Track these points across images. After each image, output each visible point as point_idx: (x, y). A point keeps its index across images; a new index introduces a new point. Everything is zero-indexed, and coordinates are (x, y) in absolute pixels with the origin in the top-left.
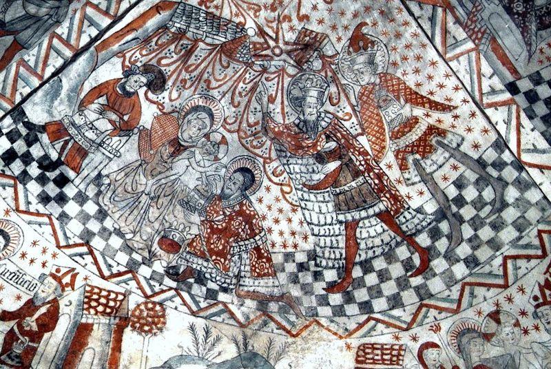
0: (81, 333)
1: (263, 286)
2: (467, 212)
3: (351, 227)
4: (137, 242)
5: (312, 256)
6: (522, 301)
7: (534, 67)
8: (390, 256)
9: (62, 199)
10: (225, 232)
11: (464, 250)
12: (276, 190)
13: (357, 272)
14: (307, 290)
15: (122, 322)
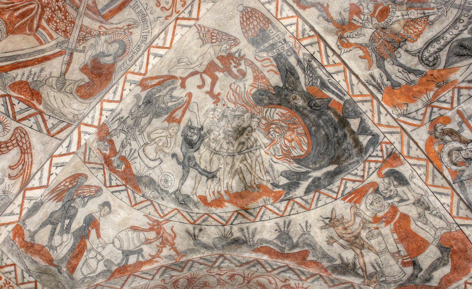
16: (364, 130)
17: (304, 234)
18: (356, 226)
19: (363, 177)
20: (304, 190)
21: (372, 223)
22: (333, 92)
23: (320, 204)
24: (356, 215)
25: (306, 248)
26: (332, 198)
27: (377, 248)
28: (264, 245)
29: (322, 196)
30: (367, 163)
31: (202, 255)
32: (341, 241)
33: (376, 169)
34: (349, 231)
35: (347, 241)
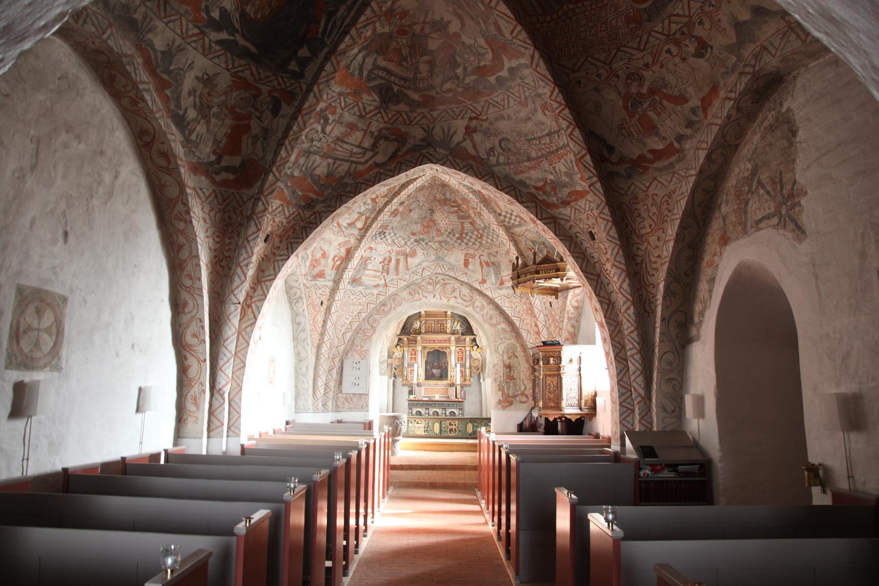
0: (398, 261)
1: (440, 239)
2: (491, 231)
3: (462, 224)
4: (405, 237)
5: (452, 230)
6: (503, 252)
7: (506, 210)
8: (472, 233)
9: (385, 237)
10: (428, 226)
11: (490, 237)
12: (440, 213)
13: (464, 235)
14: (451, 239)
15: (406, 256)
16: (303, 63)
17: (181, 69)
18: (217, 100)
19: (261, 80)
20: (219, 39)
21: (227, 109)
22: (326, 25)
23: (216, 60)
24: (226, 93)
25: (173, 82)
26: (227, 66)
27: (211, 127)
28: (148, 48)
29: (223, 57)
30: (274, 77)
31: (96, 10)
32: (198, 100)
33: (274, 87)
34: (209, 99)
35: (201, 104)
